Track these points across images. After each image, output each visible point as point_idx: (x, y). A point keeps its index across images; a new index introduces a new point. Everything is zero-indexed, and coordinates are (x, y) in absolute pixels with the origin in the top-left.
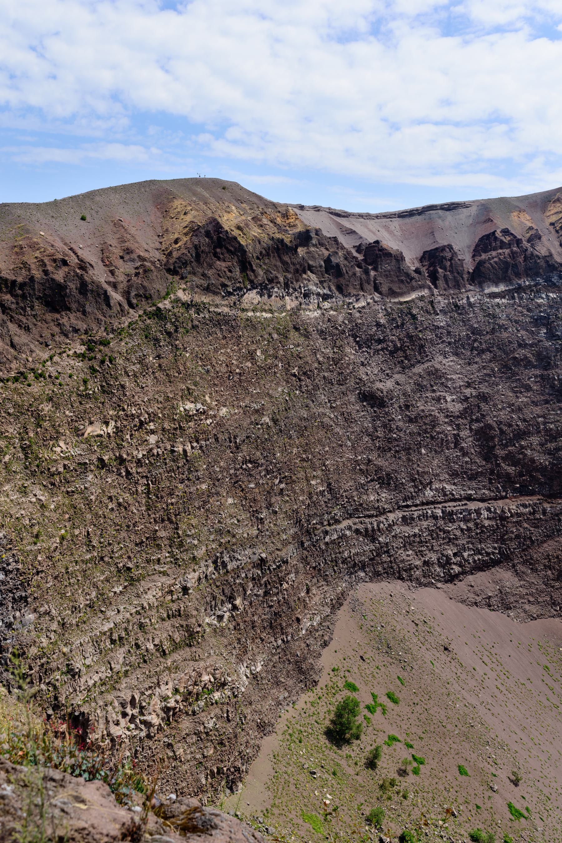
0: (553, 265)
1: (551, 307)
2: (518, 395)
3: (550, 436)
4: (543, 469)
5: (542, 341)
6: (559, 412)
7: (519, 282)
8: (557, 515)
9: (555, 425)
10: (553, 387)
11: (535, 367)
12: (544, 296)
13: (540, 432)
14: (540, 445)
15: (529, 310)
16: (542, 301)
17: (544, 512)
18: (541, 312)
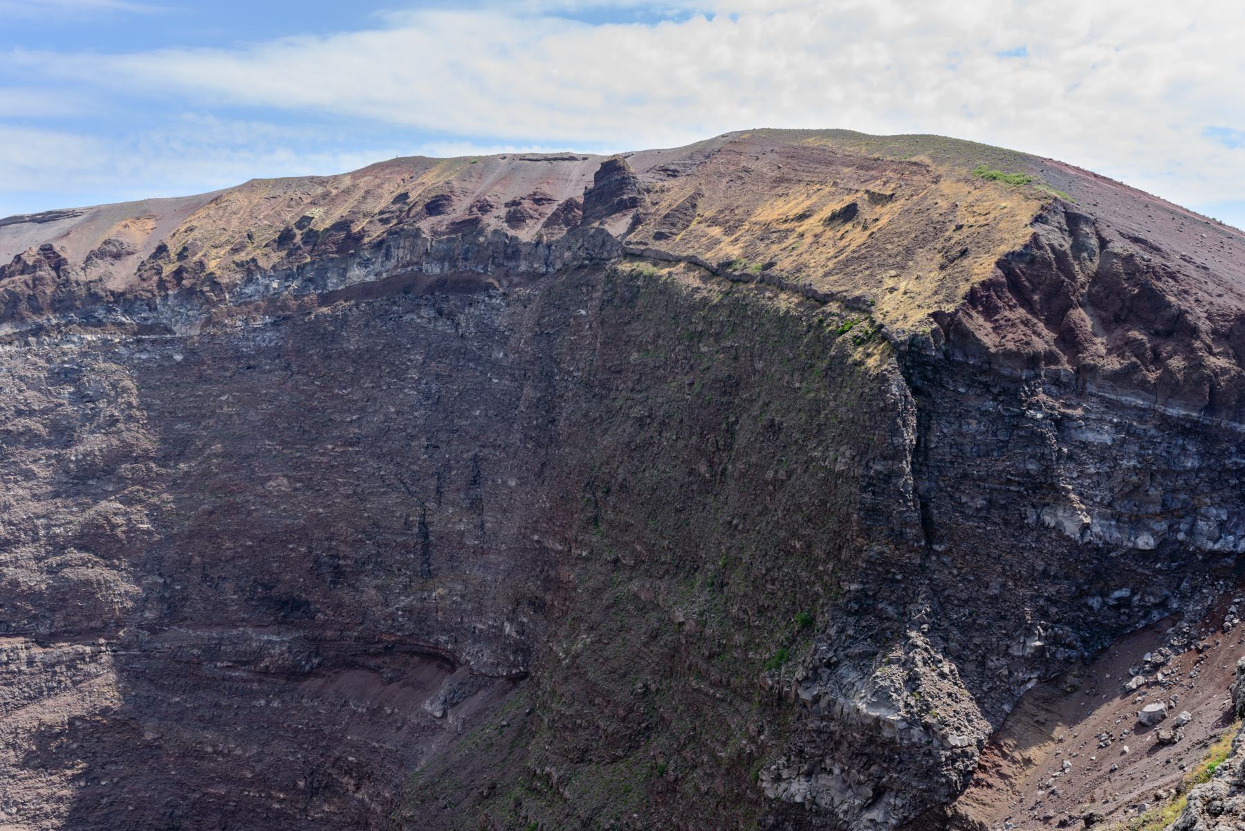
0: (96, 294)
1: (84, 354)
2: (10, 485)
3: (55, 545)
4: (33, 596)
5: (63, 405)
6: (74, 509)
7: (40, 321)
8: (53, 666)
9: (65, 528)
10: (67, 472)
11: (49, 444)
12: (75, 339)
13: (38, 540)
14: (36, 558)
15: (49, 360)
16: (72, 346)
17: (31, 662)
18: (64, 362)
